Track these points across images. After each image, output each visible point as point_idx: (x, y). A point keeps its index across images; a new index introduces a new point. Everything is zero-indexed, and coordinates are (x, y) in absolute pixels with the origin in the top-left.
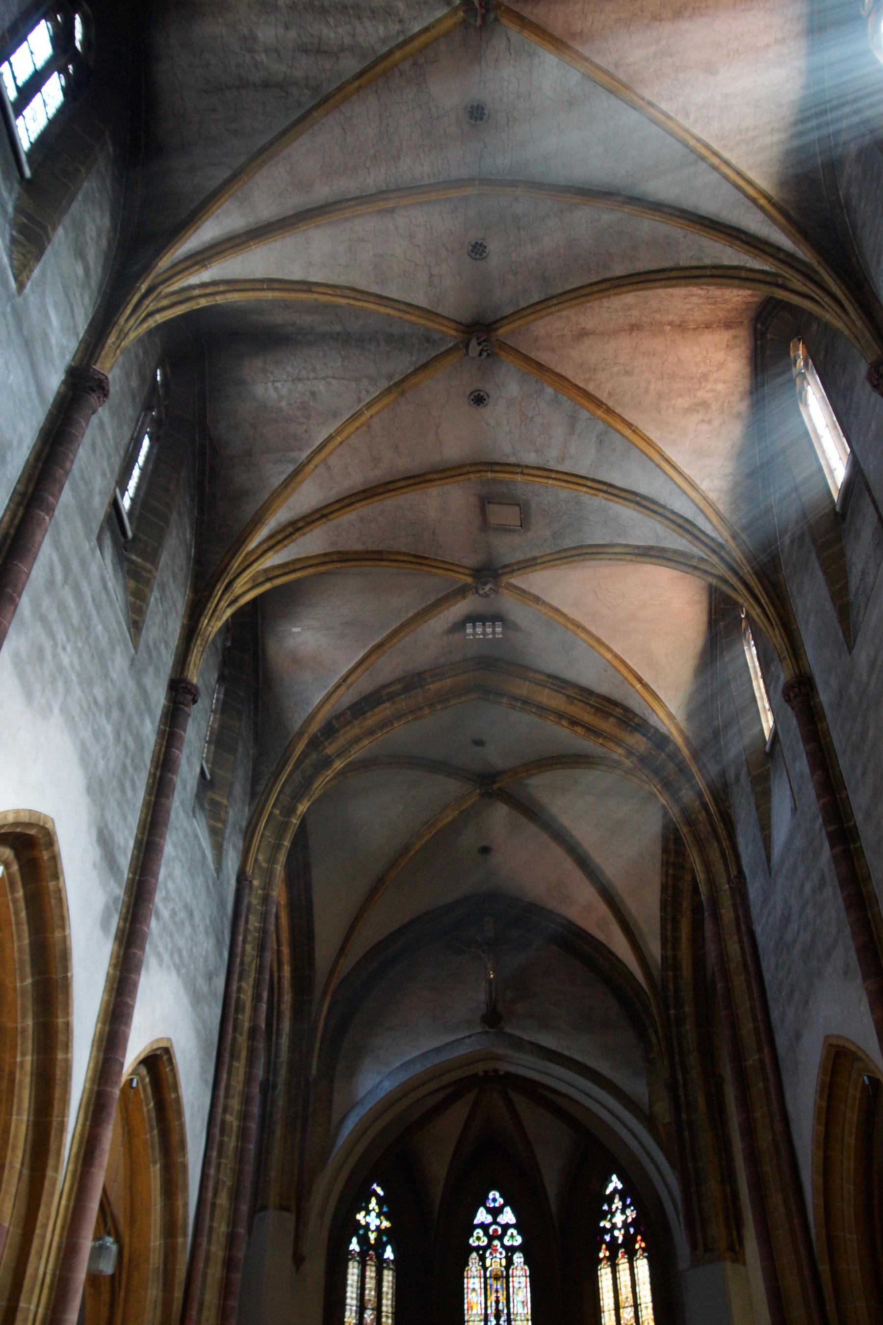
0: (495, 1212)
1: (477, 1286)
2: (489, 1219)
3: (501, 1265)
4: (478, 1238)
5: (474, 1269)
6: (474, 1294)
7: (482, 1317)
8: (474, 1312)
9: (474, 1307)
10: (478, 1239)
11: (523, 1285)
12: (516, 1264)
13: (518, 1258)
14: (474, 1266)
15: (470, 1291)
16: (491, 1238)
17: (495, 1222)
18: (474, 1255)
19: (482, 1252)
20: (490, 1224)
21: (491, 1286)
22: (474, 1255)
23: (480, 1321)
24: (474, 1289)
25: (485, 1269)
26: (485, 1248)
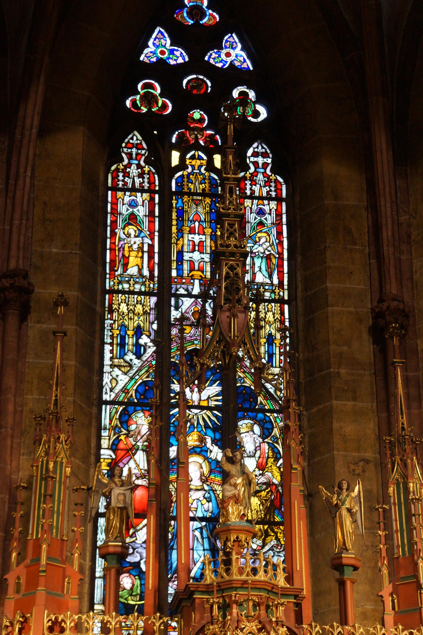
0: (198, 40)
1: (141, 211)
2: (180, 57)
3: (210, 166)
4: (149, 99)
5: (134, 171)
6: (131, 230)
7: (154, 286)
8: (133, 270)
9: (133, 261)
10: (148, 96)
11: (269, 219)
12: (252, 169)
13: (258, 156)
14: (134, 167)
15: (120, 223)
16: (185, 101)
17: (197, 63)
18: (136, 137)
19: (159, 133)
20: (183, 70)
21: (181, 213)
22: (136, 137)
23: (149, 294)
24: (132, 219)
25: (165, 171)
26: (168, 124)
